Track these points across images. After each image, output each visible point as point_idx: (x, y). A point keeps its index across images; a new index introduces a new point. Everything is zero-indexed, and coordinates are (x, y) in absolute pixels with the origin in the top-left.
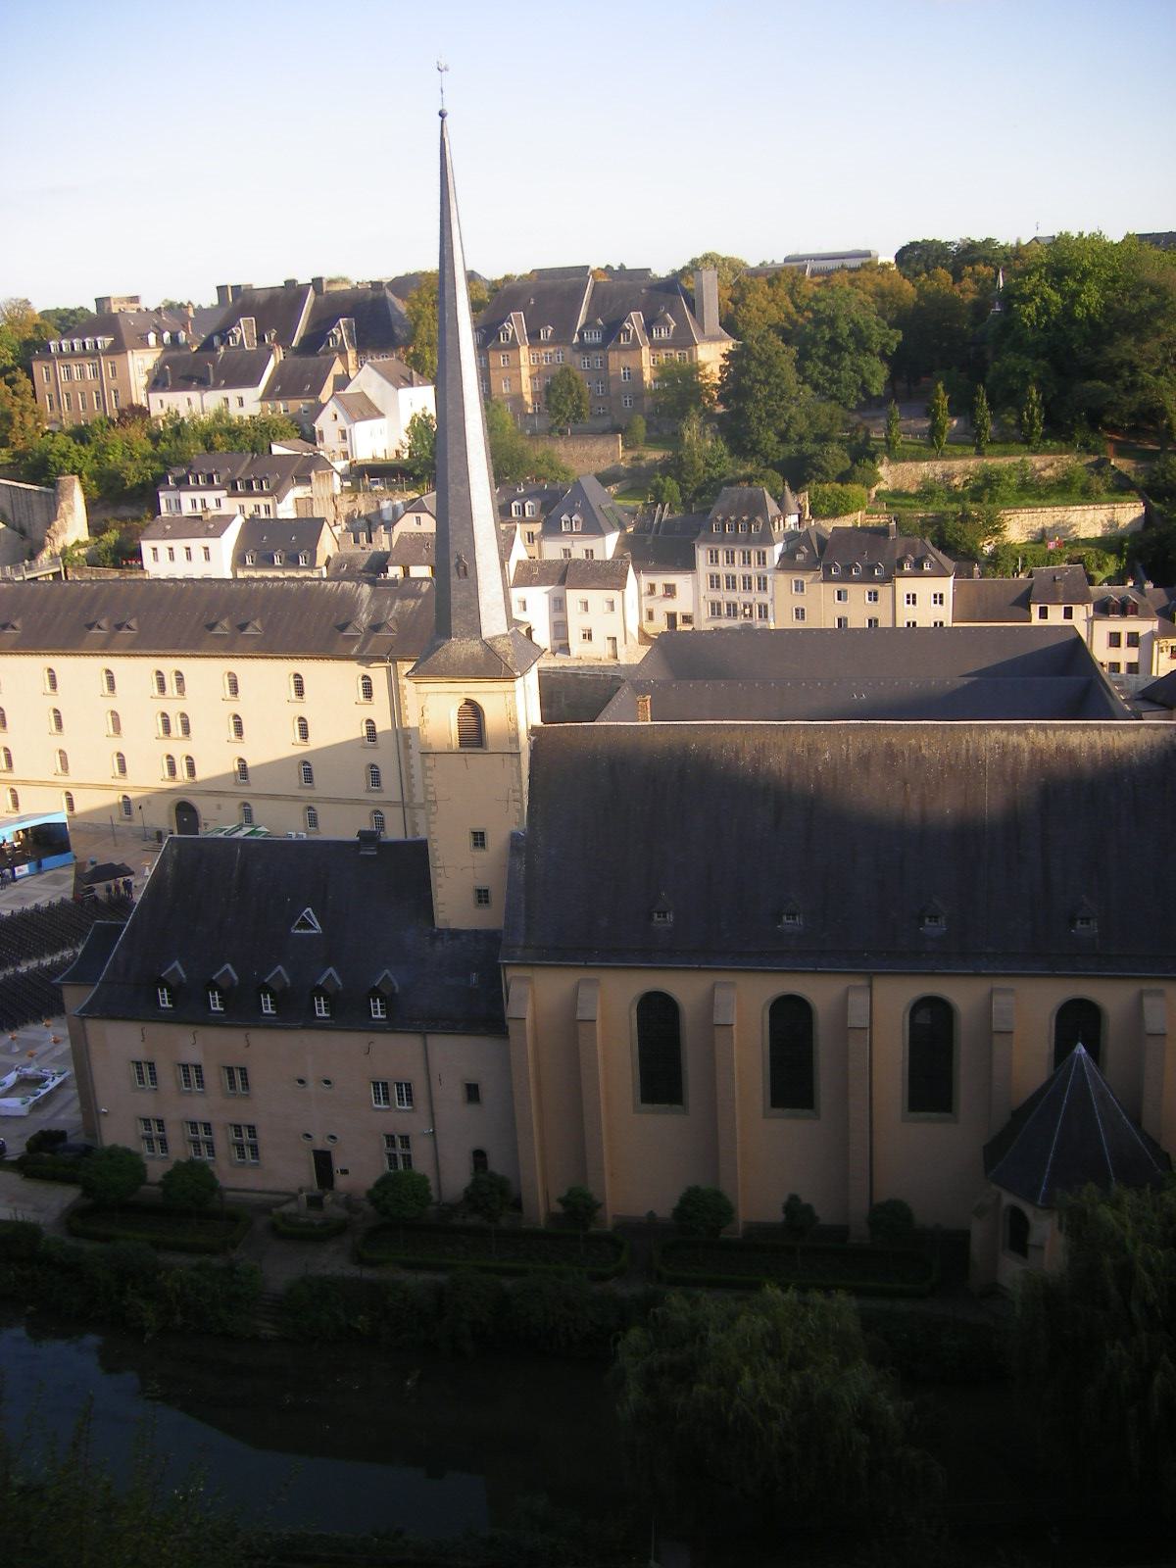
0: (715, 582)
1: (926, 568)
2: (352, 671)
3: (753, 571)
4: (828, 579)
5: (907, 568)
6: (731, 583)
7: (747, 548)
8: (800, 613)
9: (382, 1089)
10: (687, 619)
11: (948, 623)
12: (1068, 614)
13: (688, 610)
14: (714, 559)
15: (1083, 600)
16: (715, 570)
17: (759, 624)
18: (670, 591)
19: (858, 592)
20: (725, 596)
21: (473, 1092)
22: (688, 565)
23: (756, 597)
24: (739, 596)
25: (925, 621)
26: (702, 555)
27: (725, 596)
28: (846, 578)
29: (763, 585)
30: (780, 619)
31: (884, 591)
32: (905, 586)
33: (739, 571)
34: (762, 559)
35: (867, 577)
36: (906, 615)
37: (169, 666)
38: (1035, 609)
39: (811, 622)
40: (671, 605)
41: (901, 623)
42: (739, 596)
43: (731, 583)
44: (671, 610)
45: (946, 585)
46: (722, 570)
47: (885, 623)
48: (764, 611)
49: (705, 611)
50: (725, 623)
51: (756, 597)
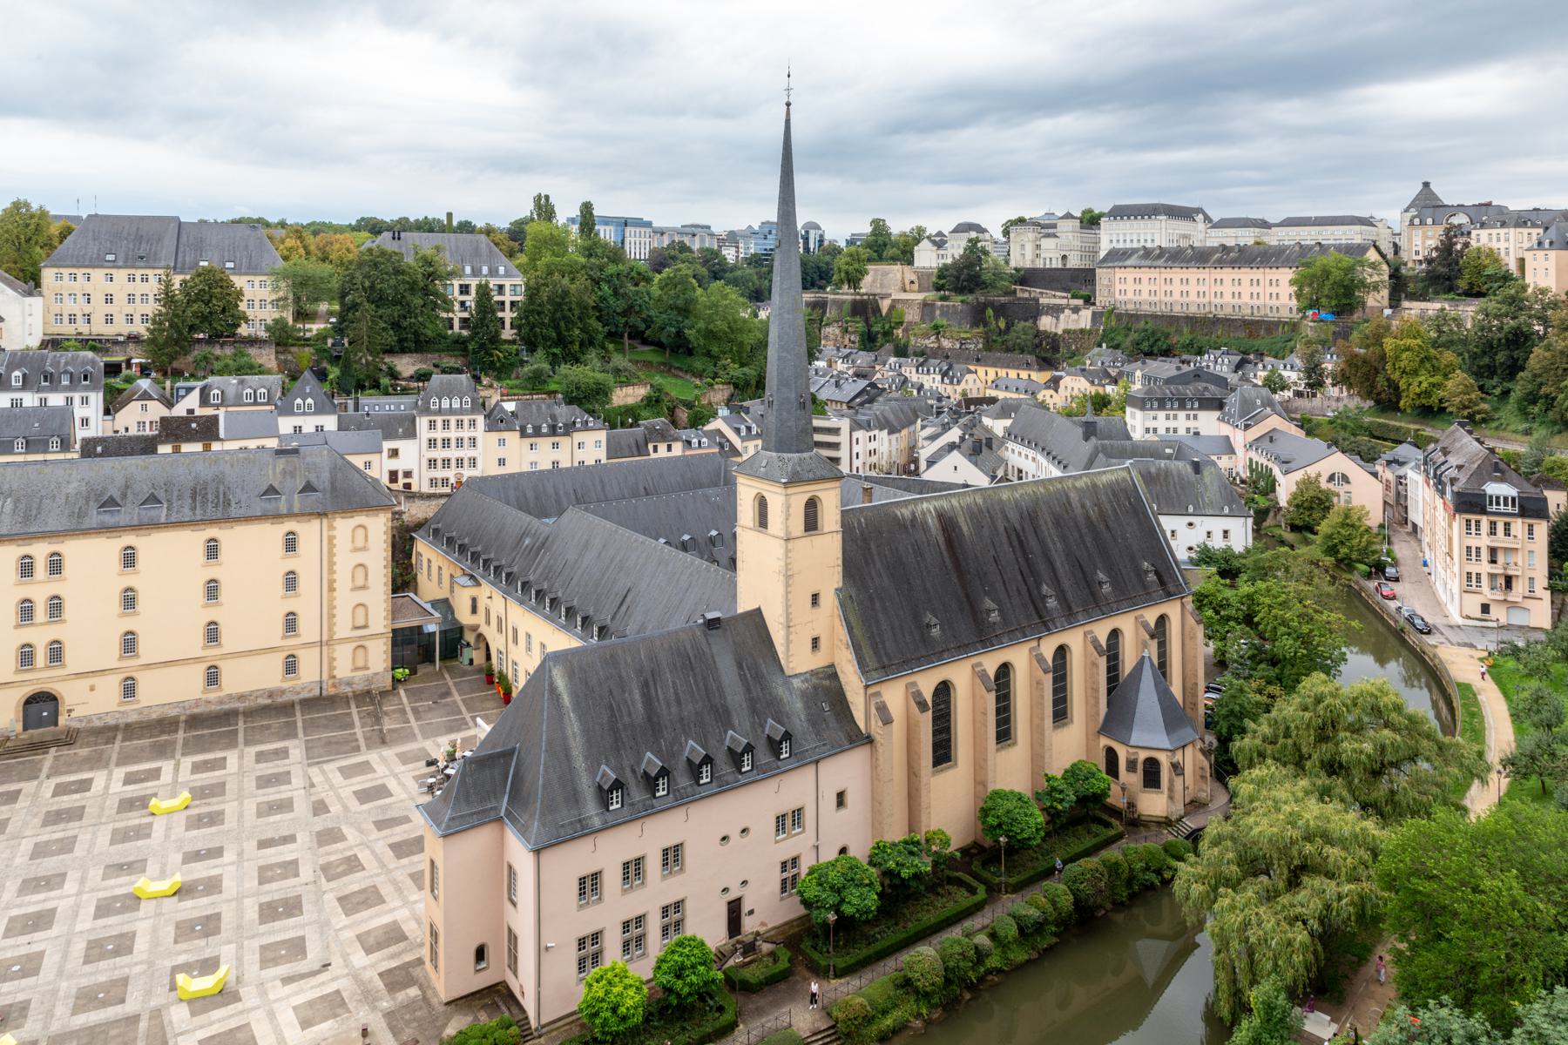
0: (432, 443)
1: (590, 425)
2: (271, 534)
3: (466, 434)
4: (523, 434)
5: (578, 425)
6: (446, 443)
7: (460, 417)
8: (502, 462)
9: (780, 821)
10: (408, 474)
11: (604, 461)
12: (669, 448)
13: (407, 468)
14: (432, 425)
15: (676, 439)
16: (432, 435)
17: (467, 473)
18: (394, 453)
19: (545, 443)
20: (439, 454)
21: (841, 799)
22: (411, 433)
23: (466, 453)
24: (453, 453)
25: (590, 462)
26: (422, 423)
27: (439, 454)
28: (537, 433)
29: (473, 441)
30: (487, 467)
31: (564, 442)
32: (578, 437)
33: (453, 434)
34: (473, 423)
35: (553, 431)
36: (580, 455)
37: (40, 551)
38: (650, 447)
39: (512, 468)
40: (394, 464)
41: (576, 464)
42: (453, 453)
43: (446, 443)
44: (393, 468)
45: (602, 436)
46: (439, 434)
47: (565, 463)
48: (473, 462)
49: (425, 463)
50: (440, 473)
51: (466, 453)
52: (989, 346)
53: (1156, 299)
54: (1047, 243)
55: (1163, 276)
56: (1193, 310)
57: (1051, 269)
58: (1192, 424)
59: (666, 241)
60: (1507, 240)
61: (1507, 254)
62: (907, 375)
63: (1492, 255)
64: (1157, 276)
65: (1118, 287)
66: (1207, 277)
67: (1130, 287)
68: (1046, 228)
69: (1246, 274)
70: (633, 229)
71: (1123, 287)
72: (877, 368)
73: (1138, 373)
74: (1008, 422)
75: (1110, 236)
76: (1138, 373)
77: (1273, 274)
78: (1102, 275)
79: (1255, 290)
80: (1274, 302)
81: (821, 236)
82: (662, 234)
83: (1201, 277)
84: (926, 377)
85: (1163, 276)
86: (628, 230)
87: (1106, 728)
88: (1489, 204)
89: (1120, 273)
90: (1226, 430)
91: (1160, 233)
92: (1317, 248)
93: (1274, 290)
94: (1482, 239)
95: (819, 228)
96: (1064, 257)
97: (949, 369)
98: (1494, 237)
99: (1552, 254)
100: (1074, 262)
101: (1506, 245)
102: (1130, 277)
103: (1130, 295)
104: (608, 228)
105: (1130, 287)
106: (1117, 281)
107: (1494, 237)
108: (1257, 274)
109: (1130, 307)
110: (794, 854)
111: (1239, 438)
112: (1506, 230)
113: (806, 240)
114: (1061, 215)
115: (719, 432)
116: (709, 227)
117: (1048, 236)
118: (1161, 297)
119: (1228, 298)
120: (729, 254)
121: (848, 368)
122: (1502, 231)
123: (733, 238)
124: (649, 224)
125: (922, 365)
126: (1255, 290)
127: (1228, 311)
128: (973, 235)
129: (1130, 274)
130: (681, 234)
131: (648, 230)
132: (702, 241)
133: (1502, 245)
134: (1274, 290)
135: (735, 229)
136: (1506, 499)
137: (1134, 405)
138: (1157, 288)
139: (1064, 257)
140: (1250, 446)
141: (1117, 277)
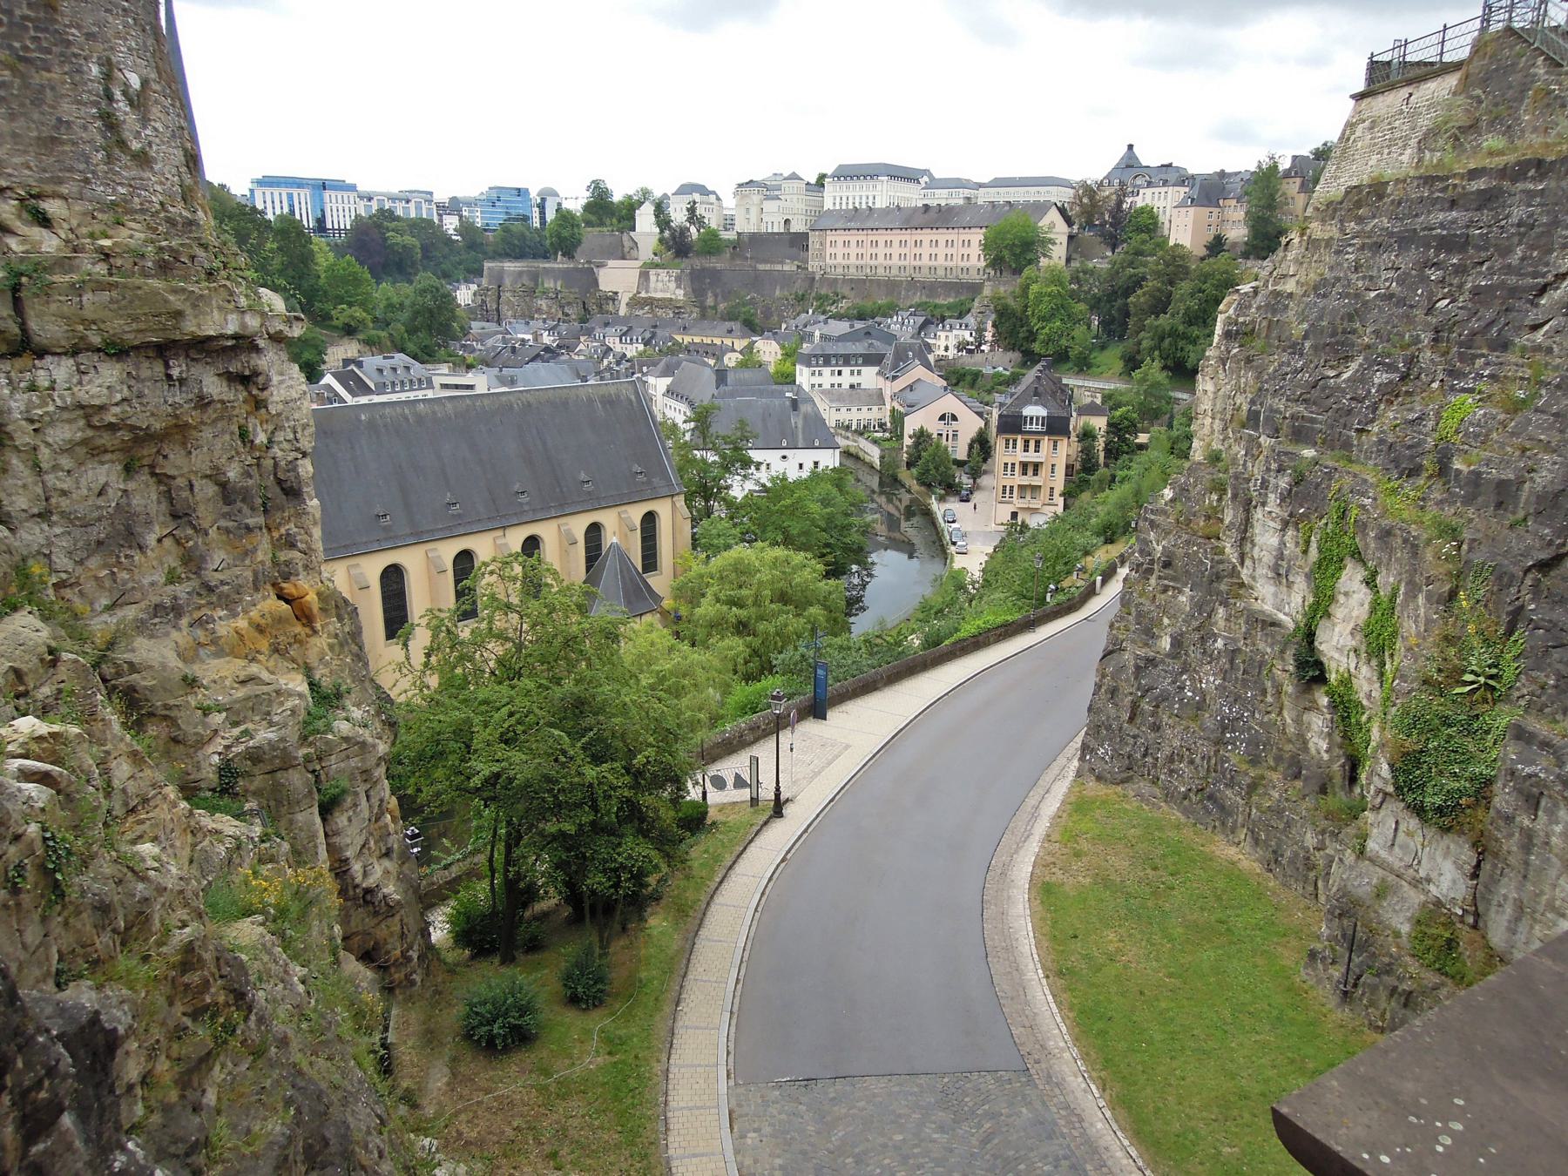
52: (703, 316)
53: (863, 262)
54: (770, 206)
57: (773, 234)
58: (855, 380)
59: (375, 206)
61: (1164, 212)
62: (611, 346)
64: (864, 238)
65: (829, 250)
66: (907, 238)
67: (840, 250)
68: (766, 189)
69: (942, 236)
70: (333, 194)
71: (833, 251)
72: (582, 339)
73: (817, 333)
74: (668, 380)
75: (832, 198)
76: (817, 333)
77: (965, 235)
78: (814, 239)
79: (950, 251)
80: (965, 264)
81: (559, 204)
82: (370, 199)
84: (629, 347)
85: (870, 238)
86: (327, 194)
88: (1170, 165)
89: (830, 236)
90: (880, 383)
91: (883, 195)
92: (1007, 208)
93: (966, 251)
95: (557, 195)
96: (787, 222)
97: (652, 338)
98: (1156, 195)
99: (1192, 210)
100: (797, 227)
101: (1161, 201)
102: (840, 240)
103: (840, 260)
104: (303, 192)
106: (828, 244)
107: (1156, 195)
108: (951, 235)
109: (840, 270)
111: (889, 389)
112: (1165, 189)
113: (542, 207)
114: (786, 175)
115: (329, 387)
116: (431, 193)
117: (768, 198)
118: (867, 261)
119: (925, 261)
120: (451, 224)
121: (554, 341)
122: (1163, 190)
123: (454, 206)
124: (352, 188)
125: (625, 334)
126: (950, 251)
127: (925, 271)
128: (697, 197)
129: (840, 237)
130: (393, 199)
131: (352, 195)
132: (418, 207)
133: (1161, 204)
134: (966, 251)
135: (459, 195)
136: (1038, 418)
137: (802, 363)
139: (787, 222)
140: (894, 396)
141: (829, 239)
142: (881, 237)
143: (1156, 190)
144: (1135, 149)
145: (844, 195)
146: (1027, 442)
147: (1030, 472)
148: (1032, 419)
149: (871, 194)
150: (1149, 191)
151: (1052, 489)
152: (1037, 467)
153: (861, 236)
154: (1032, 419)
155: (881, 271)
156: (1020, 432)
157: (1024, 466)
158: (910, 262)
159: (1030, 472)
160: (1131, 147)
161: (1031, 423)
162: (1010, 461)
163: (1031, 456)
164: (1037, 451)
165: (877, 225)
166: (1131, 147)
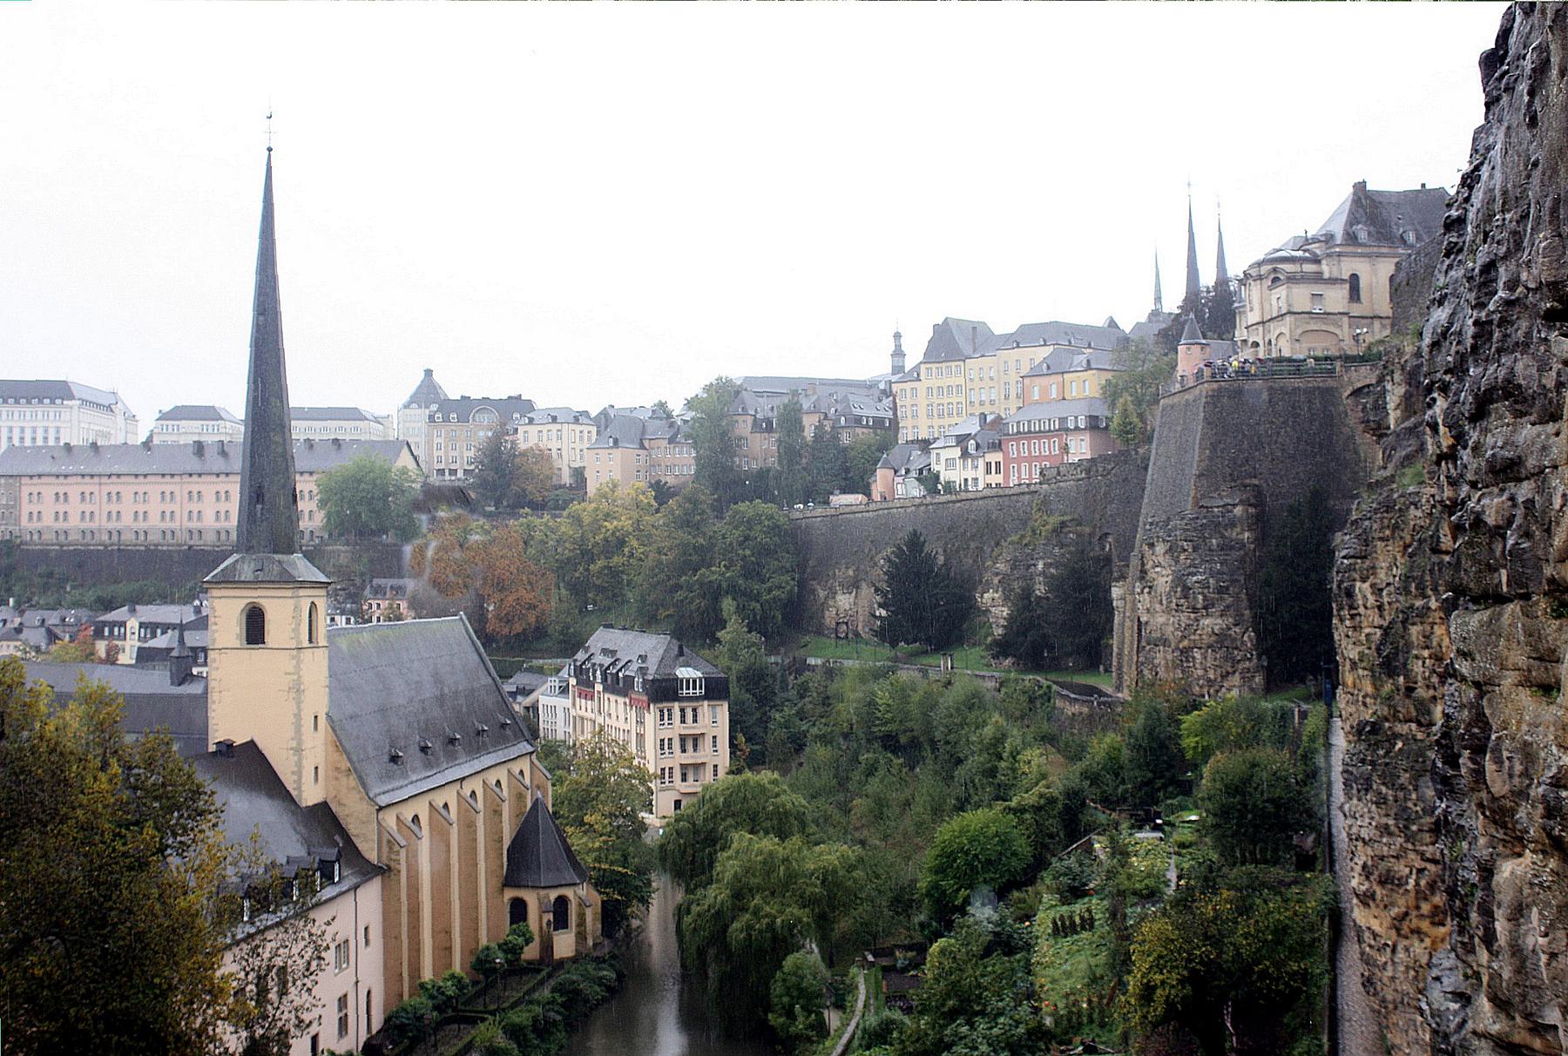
53: (94, 525)
55: (106, 490)
56: (154, 538)
60: (560, 438)
61: (560, 456)
63: (543, 456)
64: (95, 489)
66: (176, 489)
83: (168, 489)
85: (106, 490)
87: (509, 881)
94: (527, 438)
103: (48, 520)
105: (48, 508)
110: (344, 992)
118: (101, 523)
129: (49, 489)
133: (554, 445)
138: (95, 508)
141: (25, 491)
142: (127, 489)
143: (545, 428)
144: (435, 376)
145: (17, 425)
146: (682, 710)
147: (690, 746)
148: (688, 681)
149: (40, 424)
150: (533, 429)
151: (715, 766)
152: (696, 739)
153: (89, 486)
154: (682, 680)
155: (128, 537)
156: (675, 697)
157: (683, 738)
158: (181, 523)
159: (690, 746)
160: (429, 373)
161: (694, 688)
162: (666, 734)
163: (690, 729)
164: (695, 721)
165: (116, 469)
166: (429, 373)
